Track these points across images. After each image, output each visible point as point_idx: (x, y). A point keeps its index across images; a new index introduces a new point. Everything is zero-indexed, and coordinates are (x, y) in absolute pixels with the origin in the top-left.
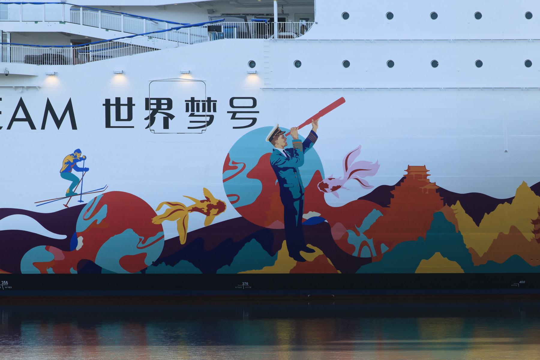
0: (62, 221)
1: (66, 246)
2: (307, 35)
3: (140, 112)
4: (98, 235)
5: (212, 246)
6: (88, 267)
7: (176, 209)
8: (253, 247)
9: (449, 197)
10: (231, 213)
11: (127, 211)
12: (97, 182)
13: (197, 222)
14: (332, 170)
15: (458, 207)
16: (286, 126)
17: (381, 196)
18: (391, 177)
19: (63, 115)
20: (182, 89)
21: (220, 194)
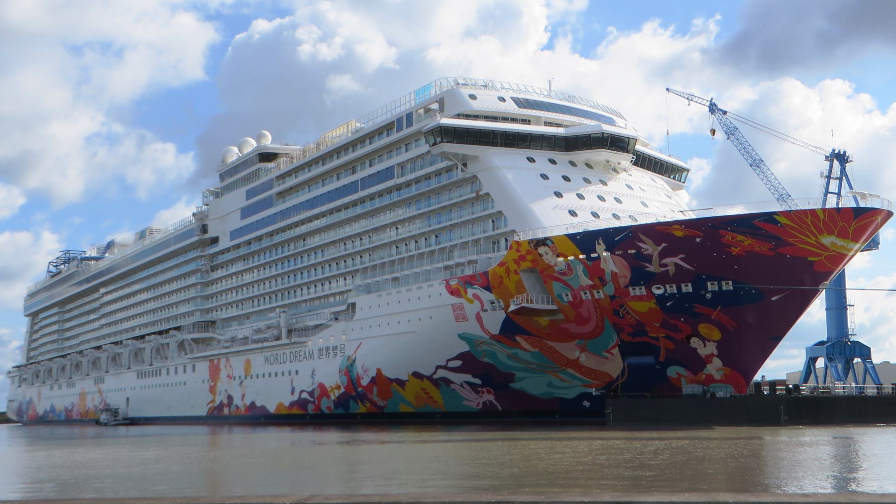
0: (311, 394)
1: (313, 403)
2: (355, 318)
3: (325, 352)
4: (320, 398)
5: (342, 401)
6: (320, 409)
7: (332, 389)
8: (352, 402)
9: (391, 381)
10: (343, 390)
11: (323, 391)
12: (319, 379)
13: (337, 394)
14: (361, 372)
15: (394, 383)
16: (351, 355)
17: (373, 381)
18: (373, 373)
19: (311, 355)
20: (332, 342)
21: (339, 383)
